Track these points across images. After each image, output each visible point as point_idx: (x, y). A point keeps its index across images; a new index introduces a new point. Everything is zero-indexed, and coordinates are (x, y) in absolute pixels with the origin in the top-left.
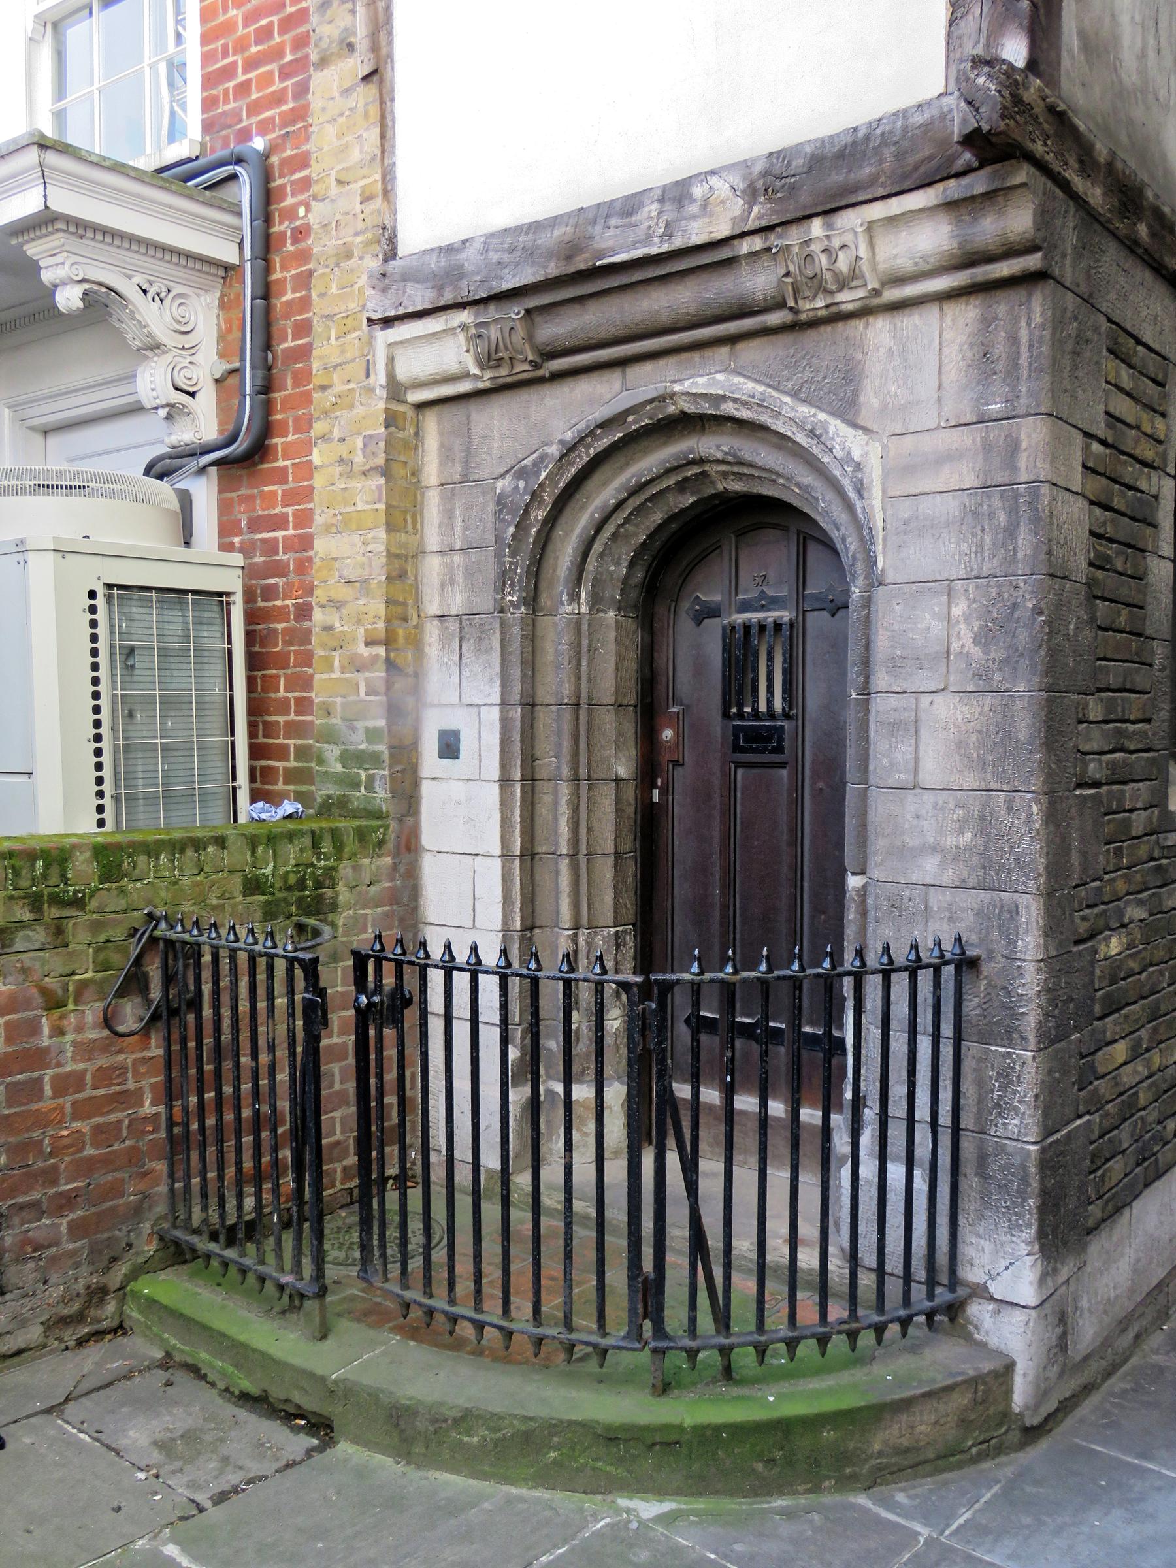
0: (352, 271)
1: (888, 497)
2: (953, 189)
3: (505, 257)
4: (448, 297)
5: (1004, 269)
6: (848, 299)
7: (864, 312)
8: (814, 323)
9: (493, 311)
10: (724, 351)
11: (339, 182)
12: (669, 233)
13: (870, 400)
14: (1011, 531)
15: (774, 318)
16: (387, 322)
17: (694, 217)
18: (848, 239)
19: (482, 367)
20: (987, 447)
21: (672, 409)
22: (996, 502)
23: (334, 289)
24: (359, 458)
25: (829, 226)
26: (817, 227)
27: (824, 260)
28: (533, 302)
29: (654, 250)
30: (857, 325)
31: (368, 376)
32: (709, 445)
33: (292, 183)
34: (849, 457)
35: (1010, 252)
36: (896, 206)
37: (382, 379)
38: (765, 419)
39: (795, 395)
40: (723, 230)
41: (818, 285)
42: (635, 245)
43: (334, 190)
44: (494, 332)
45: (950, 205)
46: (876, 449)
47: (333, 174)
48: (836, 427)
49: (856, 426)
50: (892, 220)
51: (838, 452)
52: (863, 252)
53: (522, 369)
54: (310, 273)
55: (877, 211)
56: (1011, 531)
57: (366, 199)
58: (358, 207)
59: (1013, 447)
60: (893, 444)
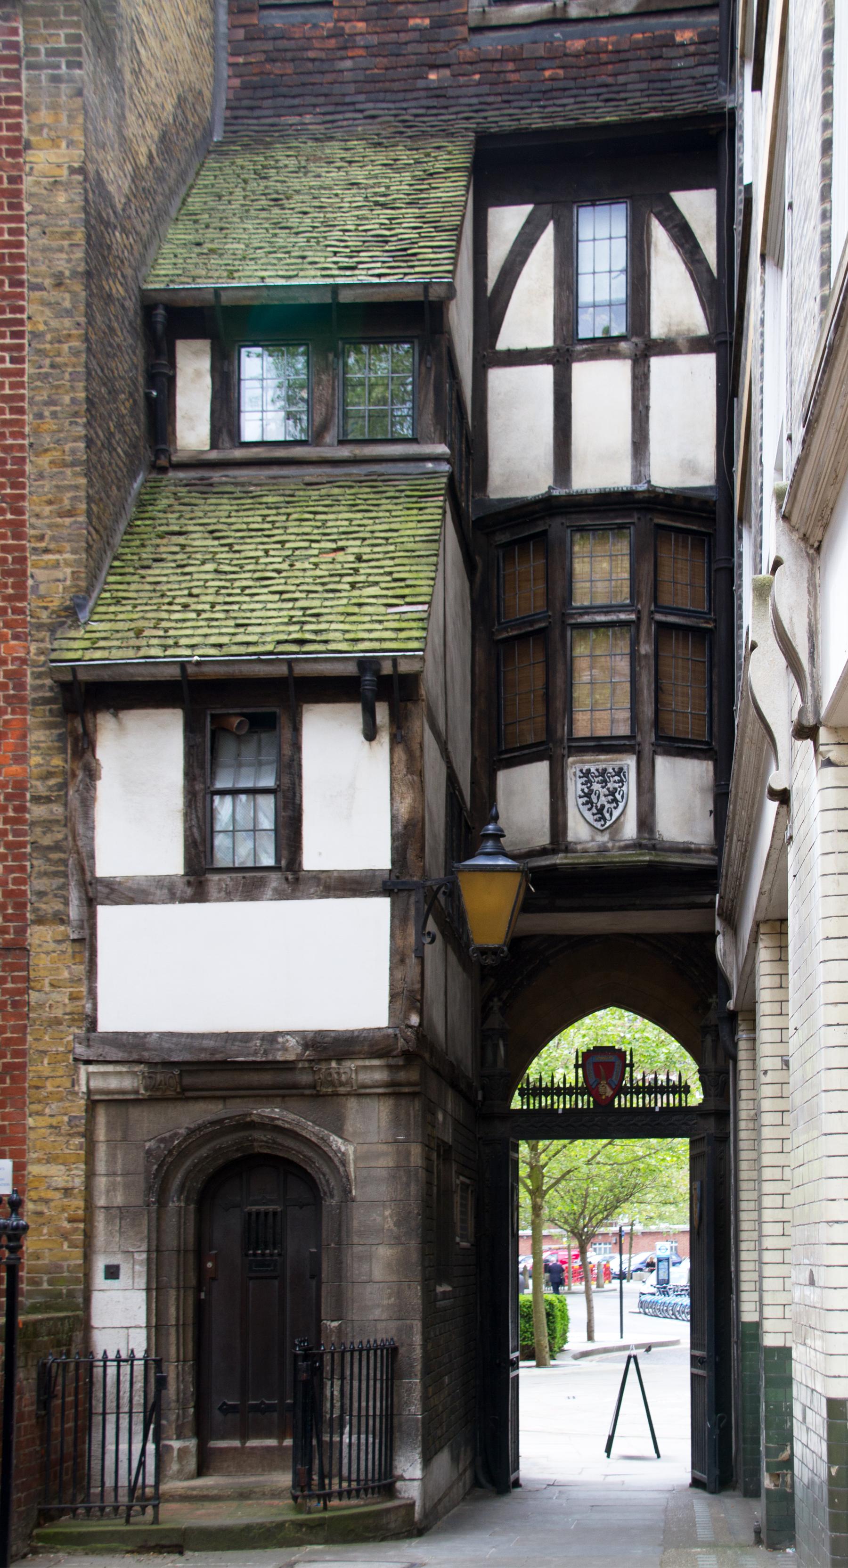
0: (62, 1032)
1: (356, 1168)
2: (392, 1061)
3: (173, 1046)
4: (135, 1056)
5: (406, 1090)
6: (342, 1090)
7: (348, 1095)
8: (325, 1095)
9: (159, 1069)
10: (279, 1099)
11: (52, 985)
12: (266, 1052)
13: (349, 1127)
14: (408, 1185)
15: (307, 1092)
16: (88, 1062)
17: (279, 1050)
18: (347, 1070)
19: (146, 1088)
20: (398, 1152)
21: (248, 1119)
22: (402, 1173)
23: (47, 1038)
24: (65, 1128)
25: (339, 1064)
26: (334, 1064)
27: (336, 1076)
28: (184, 1068)
29: (258, 1059)
30: (344, 1098)
31: (73, 1086)
32: (259, 1135)
33: (13, 977)
34: (339, 1149)
35: (409, 1084)
36: (367, 1063)
37: (84, 1089)
38: (298, 1130)
39: (313, 1122)
40: (291, 1057)
41: (332, 1083)
42: (248, 1055)
43: (47, 988)
44: (159, 1077)
45: (389, 1067)
46: (351, 1149)
47: (47, 981)
48: (333, 1138)
49: (341, 1138)
50: (365, 1067)
51: (334, 1147)
52: (353, 1076)
53: (170, 1093)
54: (25, 1026)
55: (360, 1063)
56: (408, 1185)
57: (73, 998)
58: (67, 1001)
59: (408, 1154)
60: (359, 1147)
